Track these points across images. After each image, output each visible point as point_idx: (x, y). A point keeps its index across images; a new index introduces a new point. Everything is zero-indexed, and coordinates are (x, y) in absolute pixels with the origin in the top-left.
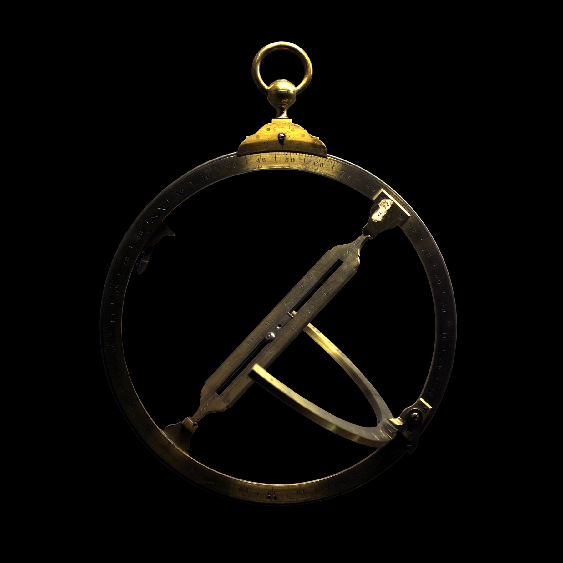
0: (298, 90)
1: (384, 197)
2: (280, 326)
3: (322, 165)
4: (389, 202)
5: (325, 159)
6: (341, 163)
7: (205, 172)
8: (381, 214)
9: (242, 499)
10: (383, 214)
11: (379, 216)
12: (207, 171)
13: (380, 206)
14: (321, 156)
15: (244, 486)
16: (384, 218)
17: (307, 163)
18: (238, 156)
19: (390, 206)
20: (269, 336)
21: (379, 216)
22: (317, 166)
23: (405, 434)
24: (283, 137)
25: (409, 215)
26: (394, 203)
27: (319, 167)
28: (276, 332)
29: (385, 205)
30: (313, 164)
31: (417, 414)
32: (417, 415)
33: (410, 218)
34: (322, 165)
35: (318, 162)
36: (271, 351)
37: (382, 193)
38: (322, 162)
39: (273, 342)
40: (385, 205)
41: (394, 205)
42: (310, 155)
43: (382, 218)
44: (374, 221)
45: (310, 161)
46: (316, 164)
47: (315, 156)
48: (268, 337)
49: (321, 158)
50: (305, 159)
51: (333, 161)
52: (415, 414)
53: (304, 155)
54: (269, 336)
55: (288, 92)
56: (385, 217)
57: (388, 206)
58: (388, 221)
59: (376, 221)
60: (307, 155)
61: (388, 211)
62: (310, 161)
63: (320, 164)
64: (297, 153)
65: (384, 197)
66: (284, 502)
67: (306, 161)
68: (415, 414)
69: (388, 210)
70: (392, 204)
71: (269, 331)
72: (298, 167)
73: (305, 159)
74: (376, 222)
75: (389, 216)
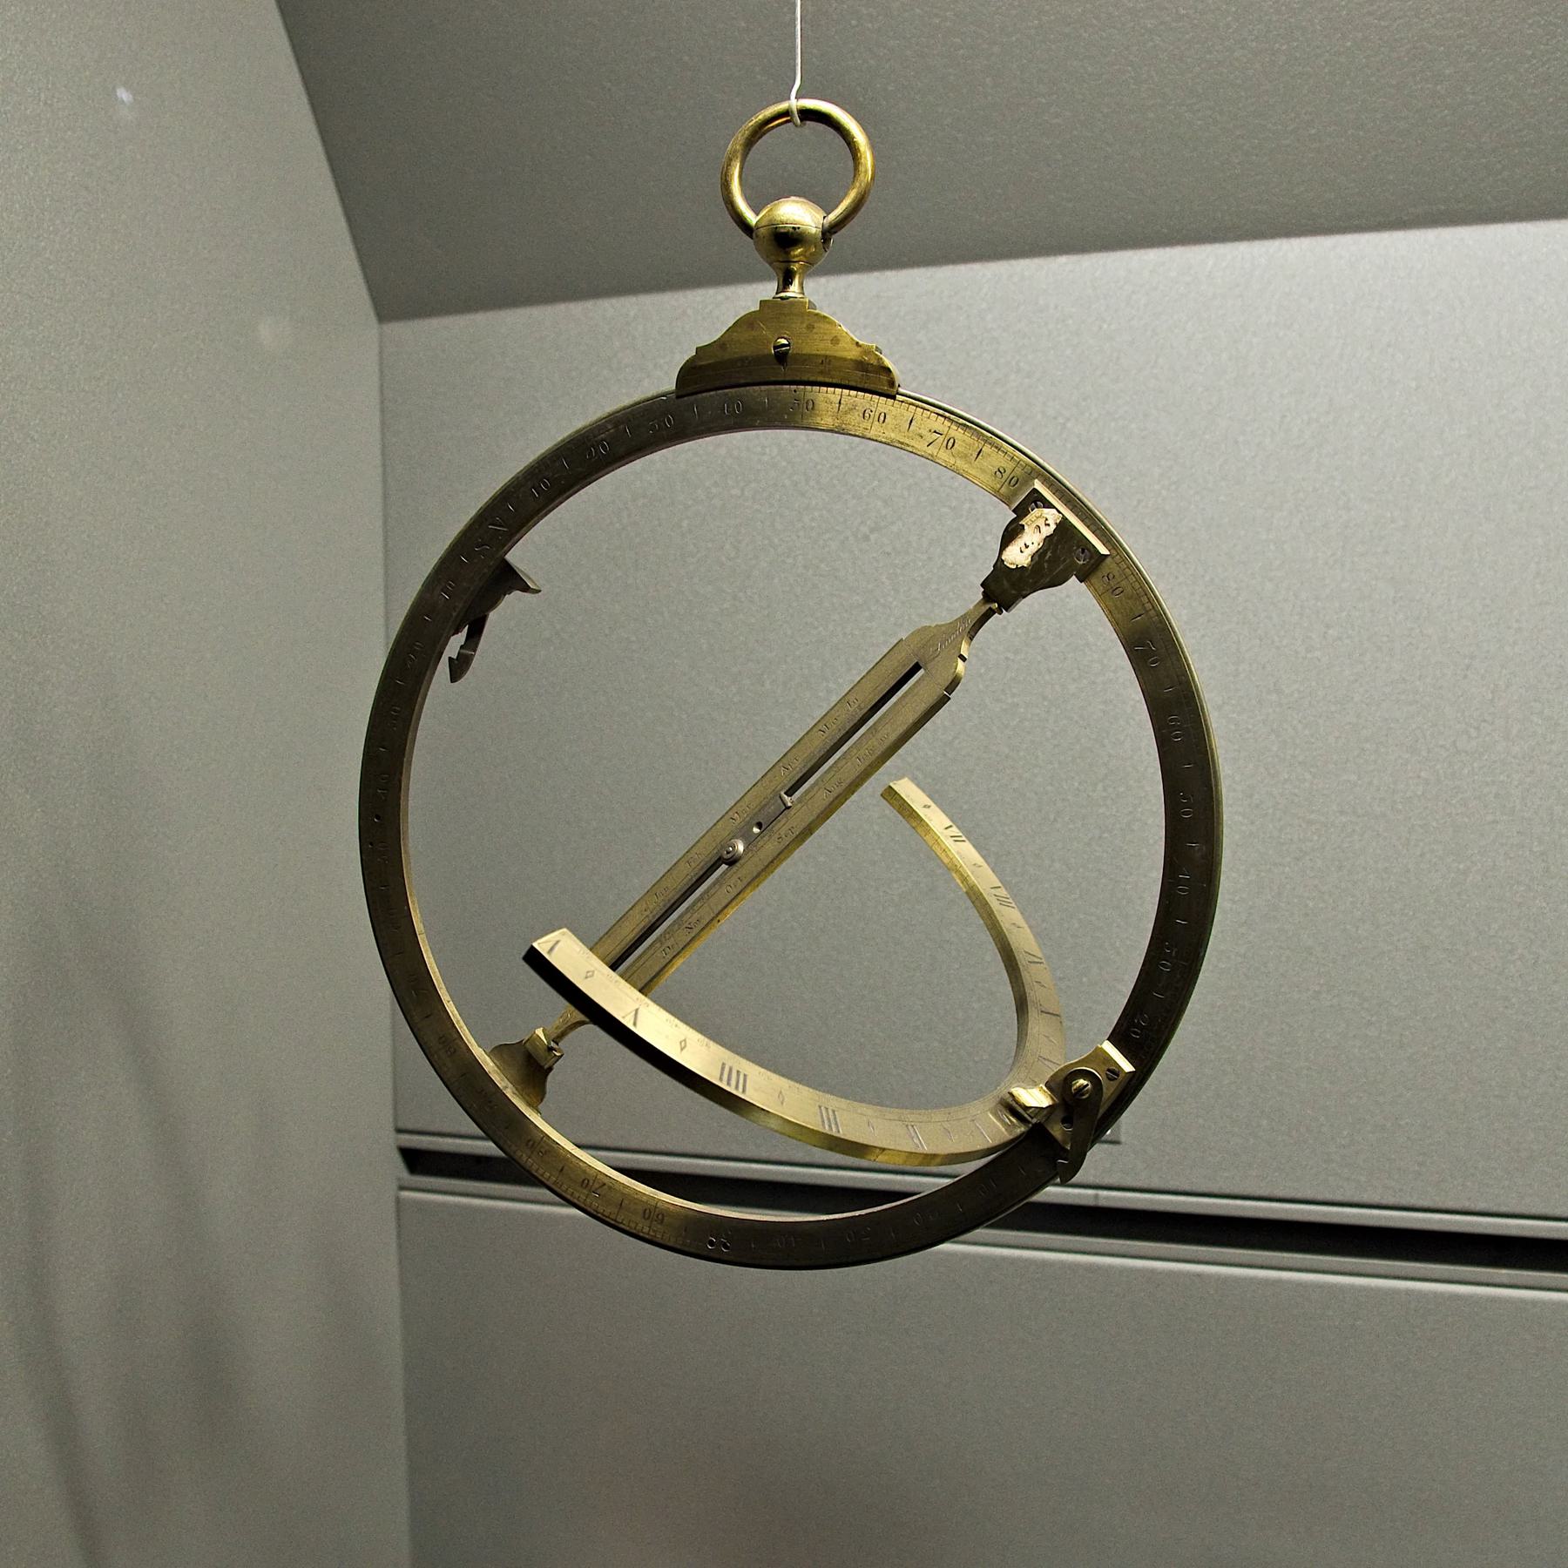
0: (830, 223)
1: (1038, 503)
2: (759, 825)
3: (882, 418)
4: (1052, 517)
5: (890, 401)
6: (910, 404)
7: (599, 437)
8: (1027, 547)
9: (647, 1237)
10: (1033, 548)
11: (1021, 552)
12: (603, 435)
13: (1026, 527)
14: (881, 394)
15: (656, 1207)
16: (1036, 558)
17: (846, 413)
18: (678, 397)
19: (1053, 527)
20: (731, 849)
21: (1021, 552)
22: (871, 420)
23: (1057, 1131)
24: (784, 345)
25: (1103, 550)
26: (1065, 518)
27: (876, 423)
28: (750, 842)
29: (1041, 522)
30: (861, 415)
31: (1085, 1083)
32: (1087, 1085)
33: (1109, 560)
34: (882, 418)
35: (874, 410)
36: (729, 888)
37: (1035, 490)
38: (882, 410)
39: (741, 862)
40: (1041, 522)
41: (1064, 526)
42: (853, 393)
43: (1030, 559)
44: (1008, 565)
45: (853, 408)
46: (867, 415)
47: (867, 395)
48: (728, 853)
49: (881, 398)
50: (840, 403)
51: (911, 406)
52: (1082, 1082)
53: (838, 391)
54: (731, 849)
55: (794, 228)
56: (1039, 556)
57: (1047, 527)
58: (1046, 565)
59: (1015, 567)
60: (846, 392)
61: (1048, 539)
62: (853, 408)
63: (877, 414)
64: (822, 388)
65: (1038, 503)
66: (648, 1234)
67: (842, 406)
68: (1082, 1082)
69: (1047, 537)
70: (1058, 521)
71: (734, 837)
72: (822, 422)
73: (840, 403)
74: (1013, 569)
75: (1049, 554)
